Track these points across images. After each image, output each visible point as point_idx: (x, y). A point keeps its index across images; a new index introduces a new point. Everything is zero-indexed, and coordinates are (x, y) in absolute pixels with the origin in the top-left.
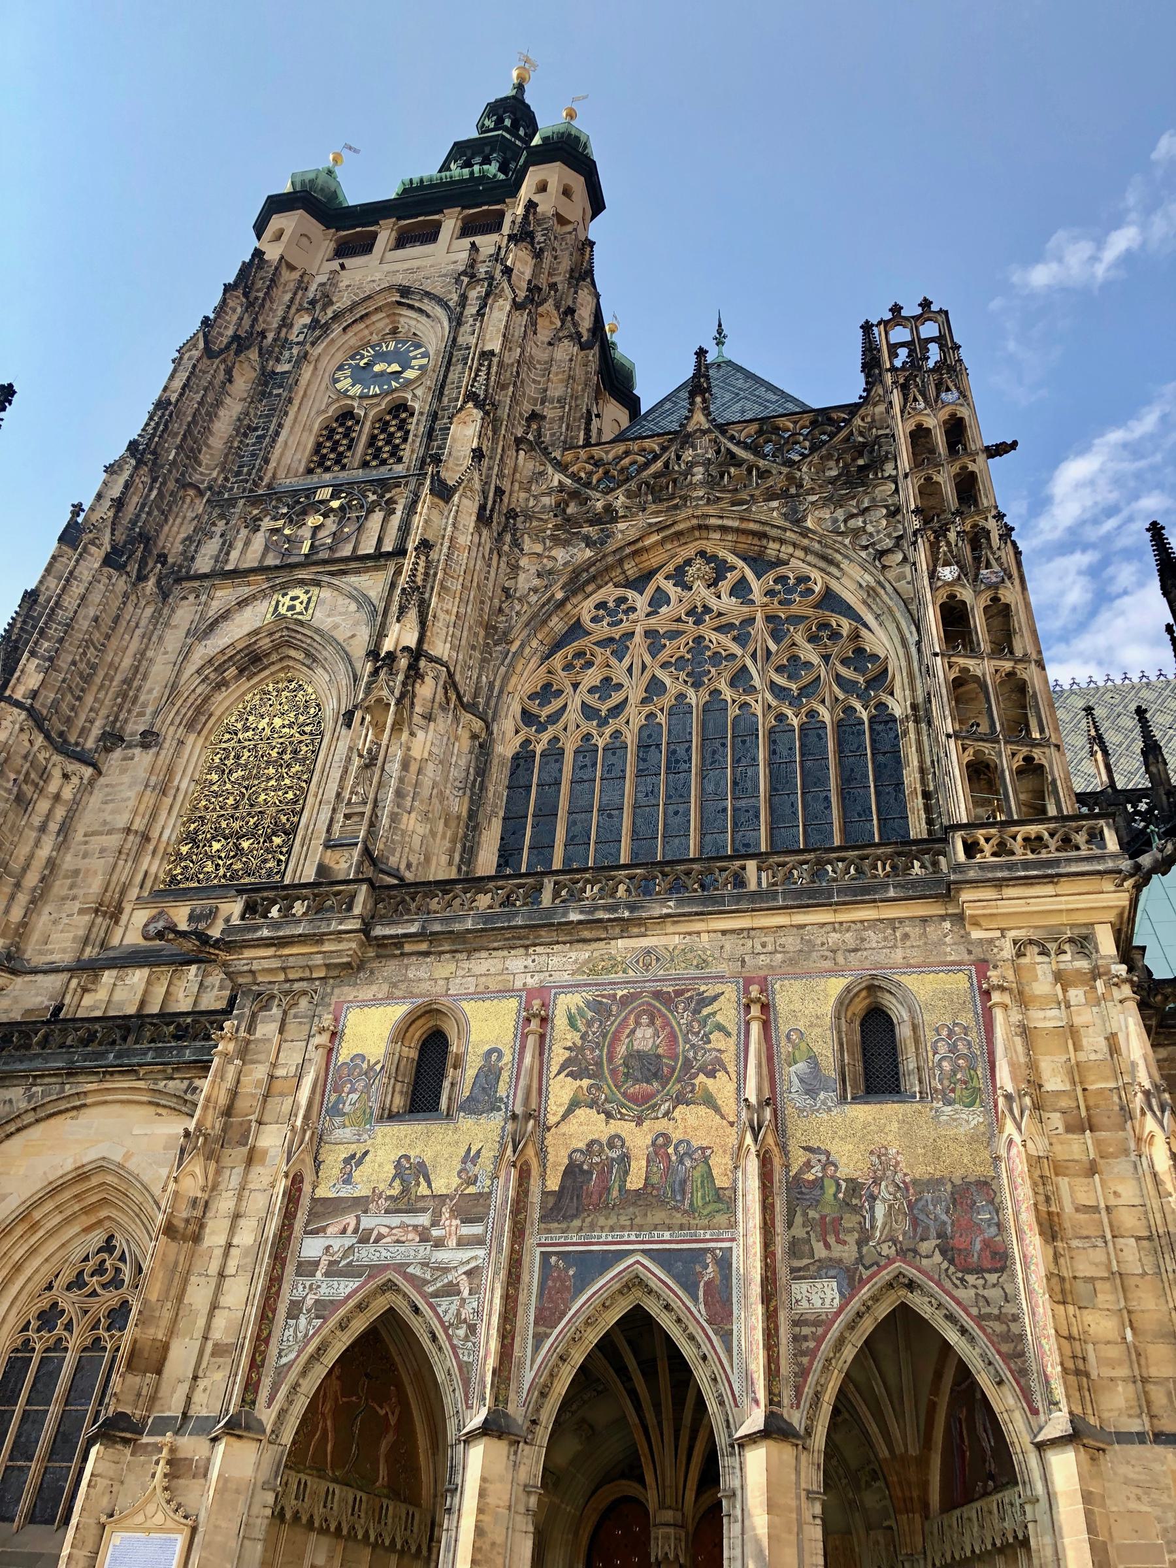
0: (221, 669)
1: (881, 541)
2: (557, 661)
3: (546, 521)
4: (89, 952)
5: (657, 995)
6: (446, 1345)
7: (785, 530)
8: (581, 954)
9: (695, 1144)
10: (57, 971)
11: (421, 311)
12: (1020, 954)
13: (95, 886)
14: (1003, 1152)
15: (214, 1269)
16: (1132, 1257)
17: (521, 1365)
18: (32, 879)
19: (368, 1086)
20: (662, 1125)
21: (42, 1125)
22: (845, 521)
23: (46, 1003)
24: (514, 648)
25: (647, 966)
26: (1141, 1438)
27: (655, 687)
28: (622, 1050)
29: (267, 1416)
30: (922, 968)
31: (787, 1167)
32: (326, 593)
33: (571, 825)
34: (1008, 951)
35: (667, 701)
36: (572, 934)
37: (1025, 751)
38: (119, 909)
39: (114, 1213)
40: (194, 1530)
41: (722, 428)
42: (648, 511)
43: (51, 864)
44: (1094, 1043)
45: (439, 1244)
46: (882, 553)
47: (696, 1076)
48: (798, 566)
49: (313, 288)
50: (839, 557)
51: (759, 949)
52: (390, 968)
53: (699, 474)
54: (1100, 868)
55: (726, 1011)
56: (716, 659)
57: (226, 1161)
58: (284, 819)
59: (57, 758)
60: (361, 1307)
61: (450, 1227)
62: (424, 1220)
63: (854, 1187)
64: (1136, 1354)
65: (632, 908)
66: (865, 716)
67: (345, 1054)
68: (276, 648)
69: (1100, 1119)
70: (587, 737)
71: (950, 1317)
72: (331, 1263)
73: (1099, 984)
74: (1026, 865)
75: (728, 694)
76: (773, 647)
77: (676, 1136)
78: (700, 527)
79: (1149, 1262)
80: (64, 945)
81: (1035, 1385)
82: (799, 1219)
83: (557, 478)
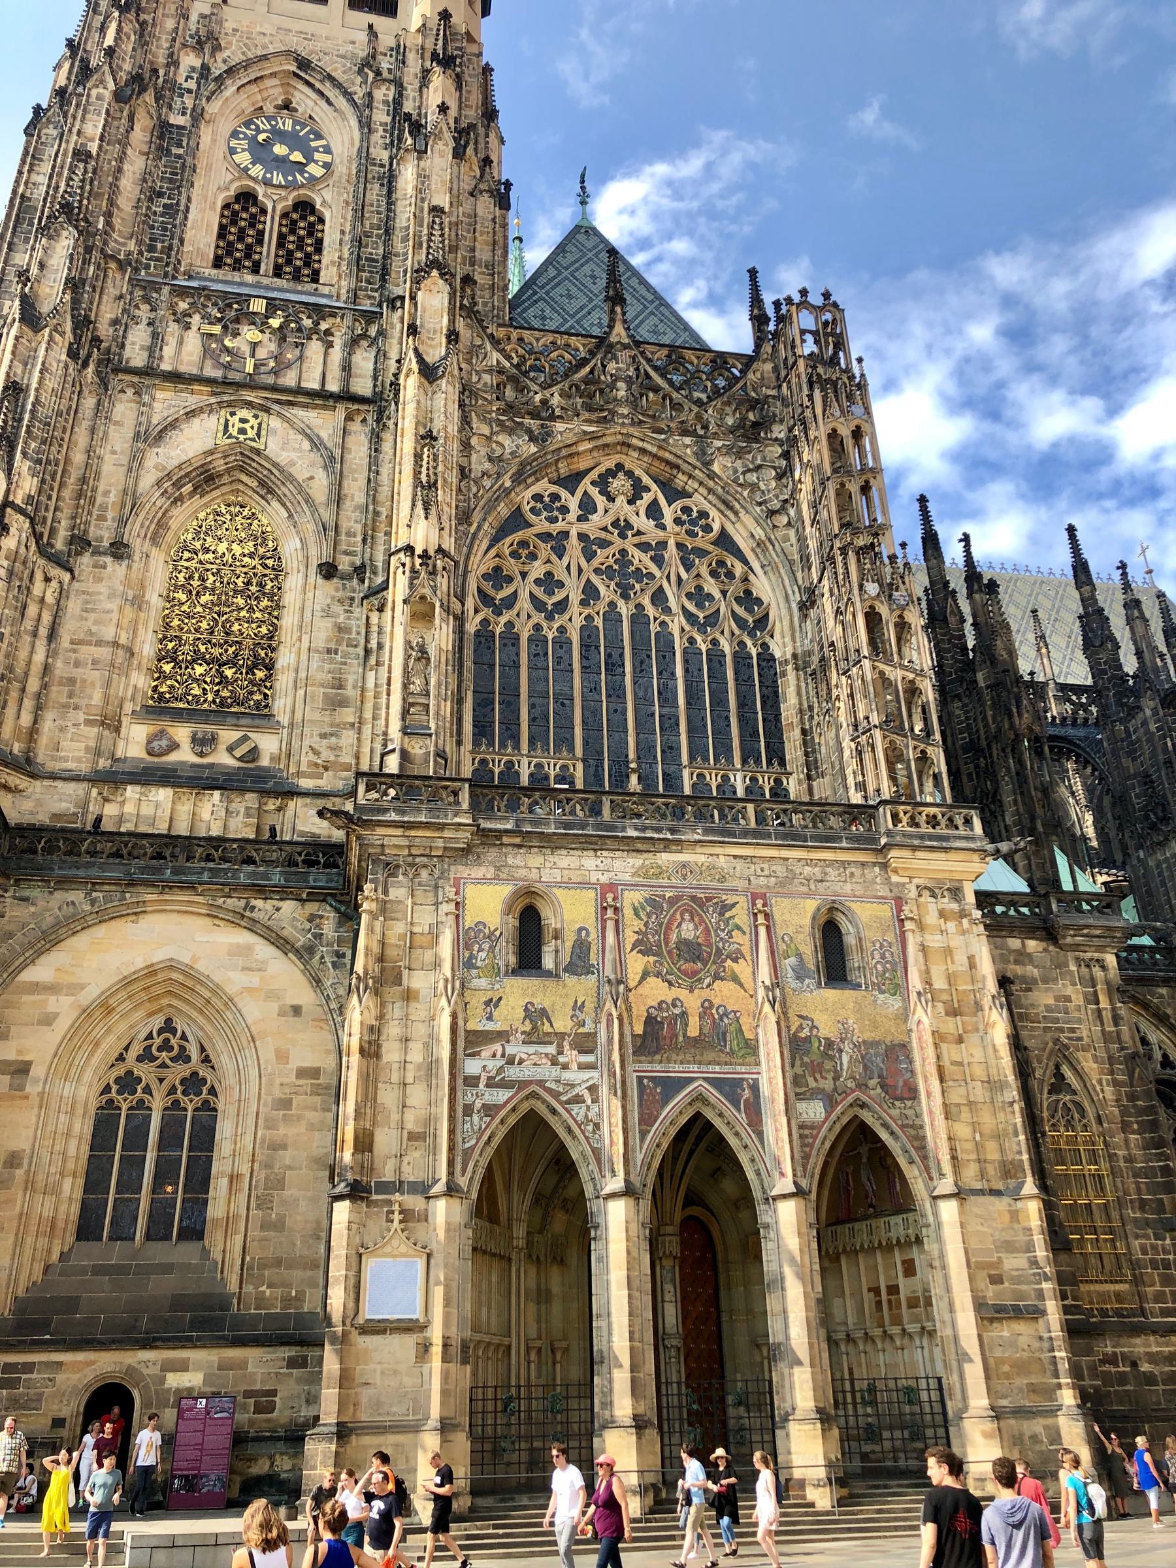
0: (178, 485)
1: (771, 500)
2: (505, 546)
3: (490, 403)
4: (103, 763)
5: (693, 898)
6: (581, 1137)
7: (695, 467)
8: (636, 861)
9: (730, 1009)
10: (76, 779)
11: (321, 93)
12: (920, 895)
13: (97, 698)
14: (914, 1028)
15: (395, 1078)
16: (979, 1093)
17: (634, 1151)
18: (33, 685)
19: (492, 948)
20: (706, 993)
21: (104, 925)
22: (744, 473)
23: (73, 810)
24: (473, 529)
25: (684, 877)
26: (981, 1192)
27: (590, 593)
28: (674, 937)
29: (463, 1182)
30: (862, 898)
31: (788, 1027)
32: (275, 422)
33: (532, 706)
34: (913, 893)
35: (602, 607)
36: (630, 846)
37: (923, 746)
38: (120, 722)
39: (175, 1002)
40: (429, 1256)
41: (638, 344)
42: (582, 418)
43: (47, 669)
44: (961, 959)
45: (565, 1067)
46: (772, 513)
47: (724, 961)
48: (699, 501)
49: (194, 17)
50: (737, 506)
51: (759, 872)
52: (492, 854)
53: (622, 391)
54: (973, 846)
55: (741, 915)
56: (639, 575)
57: (388, 998)
58: (262, 653)
59: (41, 562)
60: (514, 1109)
61: (571, 1056)
62: (551, 1049)
63: (830, 1044)
64: (979, 1147)
65: (673, 831)
66: (754, 652)
67: (469, 922)
68: (228, 471)
69: (965, 1009)
70: (537, 627)
71: (885, 1125)
72: (489, 1078)
73: (965, 921)
74: (931, 838)
75: (651, 611)
76: (684, 575)
77: (716, 1002)
78: (623, 444)
79: (988, 1094)
80: (77, 754)
81: (931, 1165)
82: (798, 1062)
83: (495, 357)
